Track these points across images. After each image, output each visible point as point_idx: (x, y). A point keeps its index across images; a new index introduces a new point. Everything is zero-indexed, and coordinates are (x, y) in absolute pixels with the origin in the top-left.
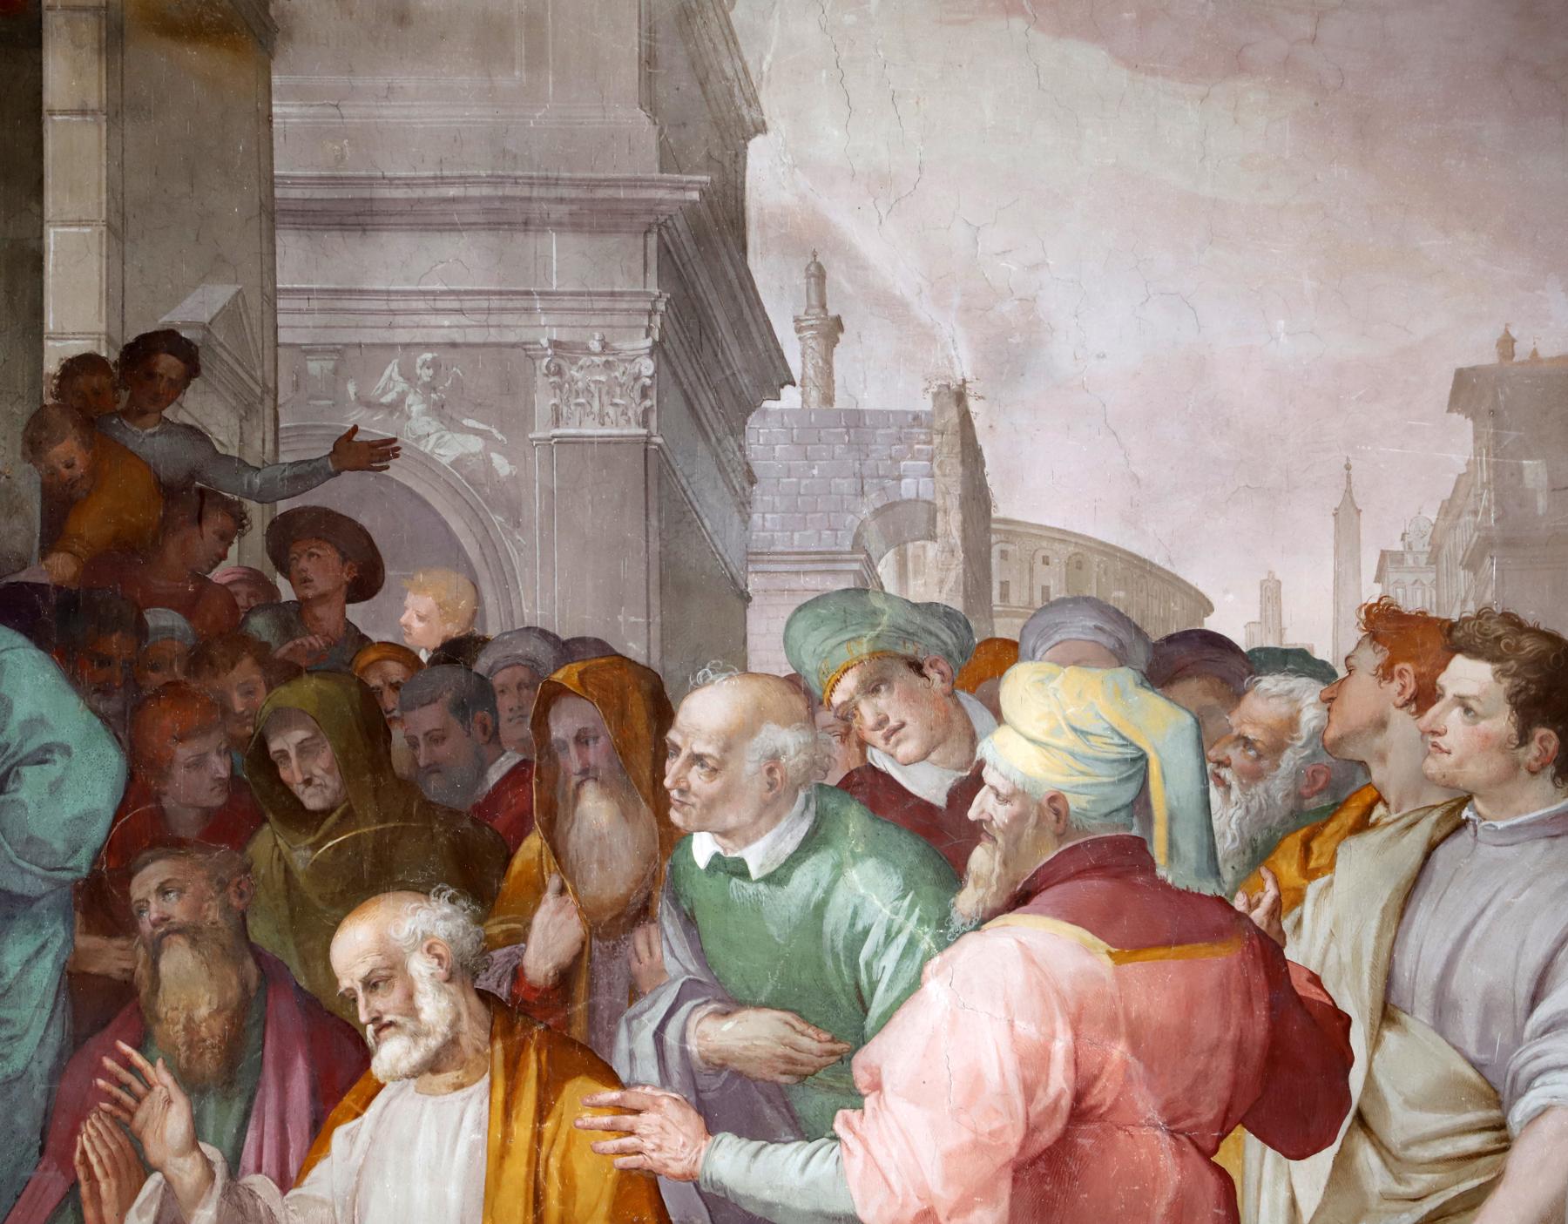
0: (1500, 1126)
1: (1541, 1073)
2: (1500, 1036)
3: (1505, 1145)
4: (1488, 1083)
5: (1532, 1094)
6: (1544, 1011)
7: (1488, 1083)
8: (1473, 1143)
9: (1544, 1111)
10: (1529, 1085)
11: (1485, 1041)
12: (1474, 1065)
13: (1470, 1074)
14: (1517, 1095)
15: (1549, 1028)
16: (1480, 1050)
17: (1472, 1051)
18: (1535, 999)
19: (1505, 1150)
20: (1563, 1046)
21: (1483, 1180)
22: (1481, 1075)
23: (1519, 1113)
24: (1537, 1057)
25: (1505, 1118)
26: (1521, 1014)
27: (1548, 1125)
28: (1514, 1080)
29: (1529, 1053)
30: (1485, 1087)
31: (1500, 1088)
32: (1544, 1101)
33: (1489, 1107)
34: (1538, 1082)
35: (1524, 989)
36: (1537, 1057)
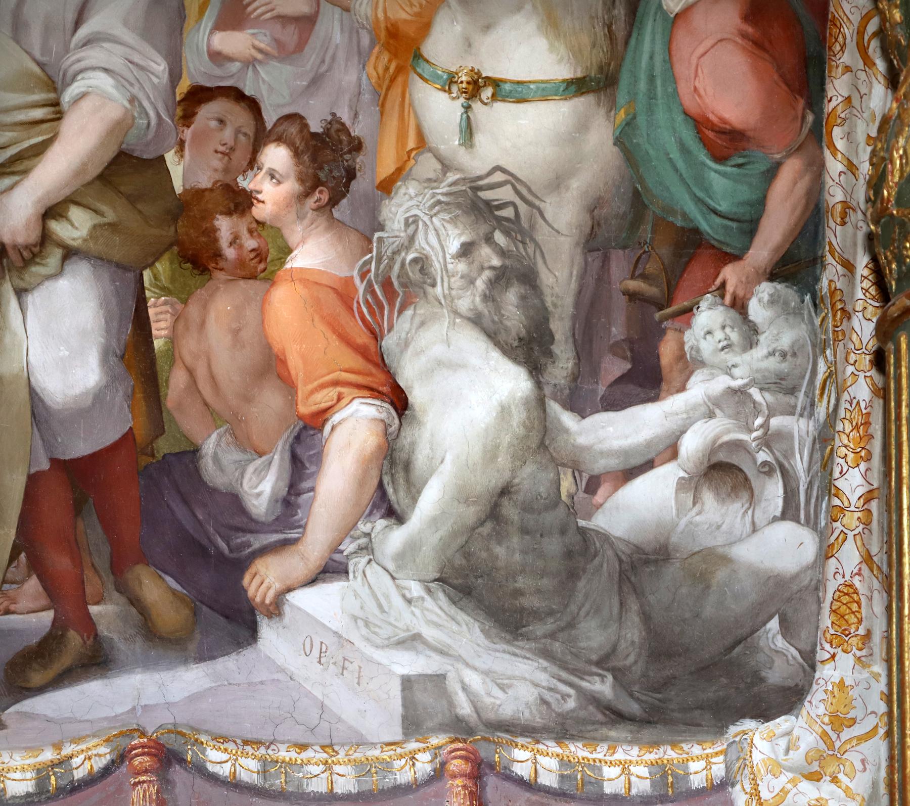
0: (56, 104)
1: (81, 71)
2: (55, 46)
3: (59, 116)
4: (47, 75)
5: (76, 84)
6: (83, 32)
7: (47, 75)
8: (38, 114)
9: (83, 95)
10: (74, 78)
11: (45, 49)
12: (39, 64)
13: (37, 70)
14: (66, 85)
15: (87, 42)
16: (42, 55)
17: (38, 55)
18: (77, 24)
19: (59, 119)
20: (94, 55)
21: (45, 137)
22: (43, 70)
23: (67, 97)
24: (79, 61)
25: (59, 98)
26: (69, 33)
27: (86, 105)
28: (64, 75)
29: (74, 58)
30: (46, 78)
31: (56, 80)
32: (83, 89)
33: (49, 91)
34: (79, 77)
35: (71, 16)
36: (79, 61)
